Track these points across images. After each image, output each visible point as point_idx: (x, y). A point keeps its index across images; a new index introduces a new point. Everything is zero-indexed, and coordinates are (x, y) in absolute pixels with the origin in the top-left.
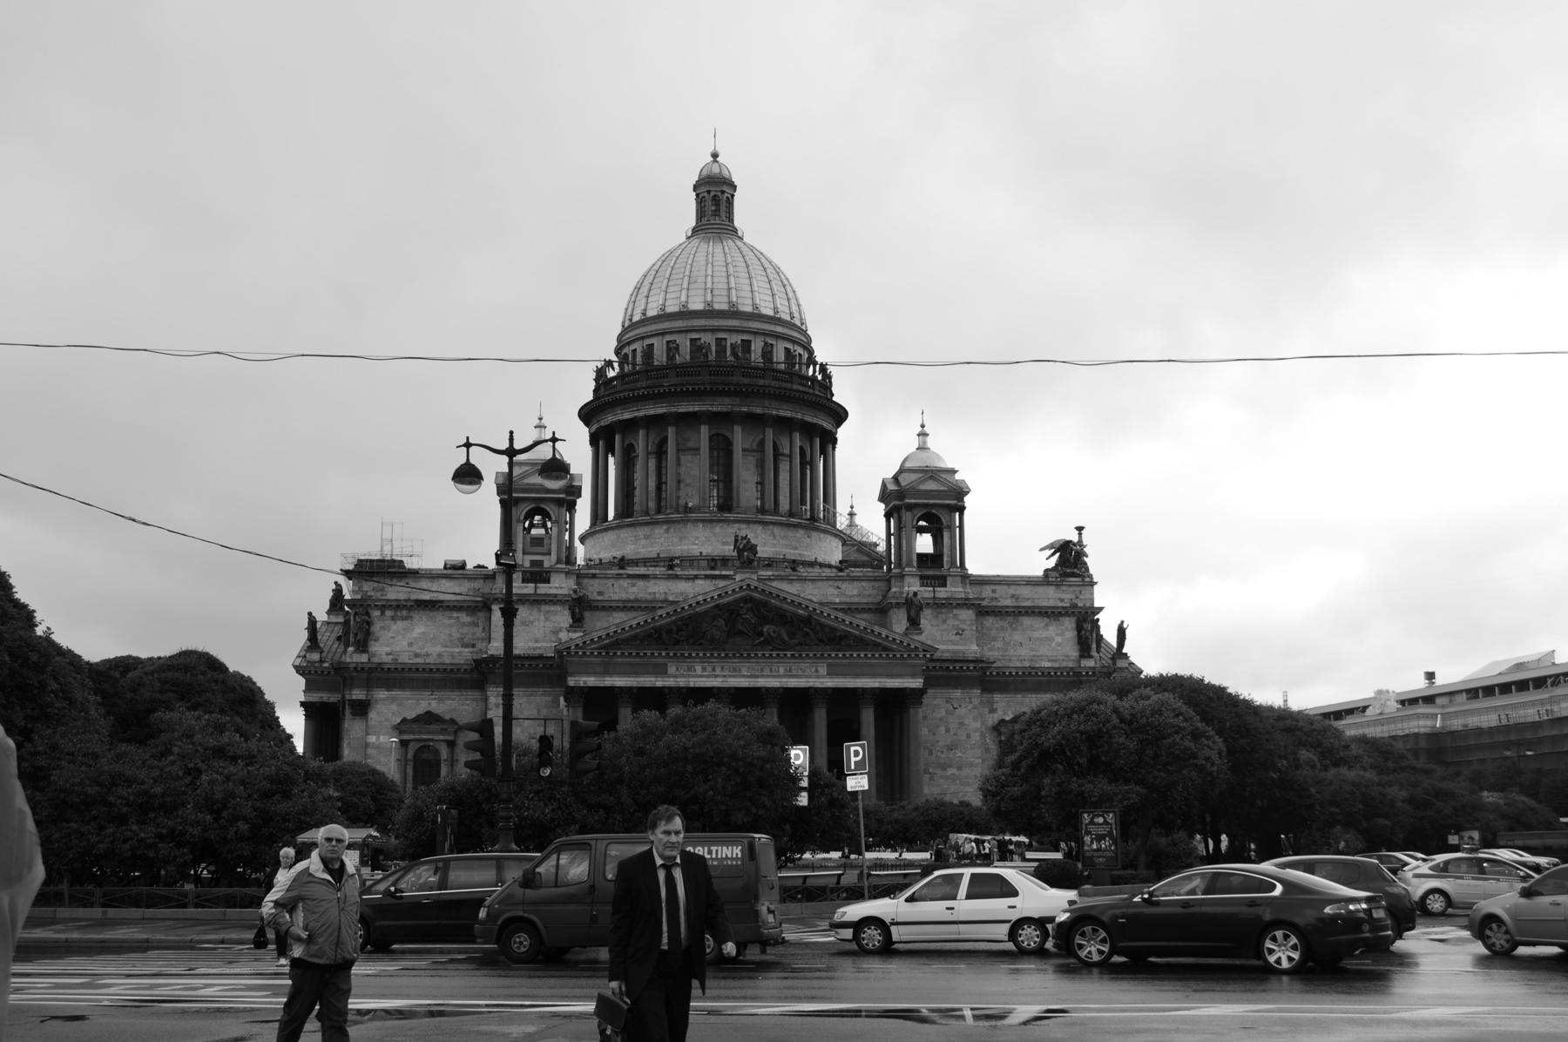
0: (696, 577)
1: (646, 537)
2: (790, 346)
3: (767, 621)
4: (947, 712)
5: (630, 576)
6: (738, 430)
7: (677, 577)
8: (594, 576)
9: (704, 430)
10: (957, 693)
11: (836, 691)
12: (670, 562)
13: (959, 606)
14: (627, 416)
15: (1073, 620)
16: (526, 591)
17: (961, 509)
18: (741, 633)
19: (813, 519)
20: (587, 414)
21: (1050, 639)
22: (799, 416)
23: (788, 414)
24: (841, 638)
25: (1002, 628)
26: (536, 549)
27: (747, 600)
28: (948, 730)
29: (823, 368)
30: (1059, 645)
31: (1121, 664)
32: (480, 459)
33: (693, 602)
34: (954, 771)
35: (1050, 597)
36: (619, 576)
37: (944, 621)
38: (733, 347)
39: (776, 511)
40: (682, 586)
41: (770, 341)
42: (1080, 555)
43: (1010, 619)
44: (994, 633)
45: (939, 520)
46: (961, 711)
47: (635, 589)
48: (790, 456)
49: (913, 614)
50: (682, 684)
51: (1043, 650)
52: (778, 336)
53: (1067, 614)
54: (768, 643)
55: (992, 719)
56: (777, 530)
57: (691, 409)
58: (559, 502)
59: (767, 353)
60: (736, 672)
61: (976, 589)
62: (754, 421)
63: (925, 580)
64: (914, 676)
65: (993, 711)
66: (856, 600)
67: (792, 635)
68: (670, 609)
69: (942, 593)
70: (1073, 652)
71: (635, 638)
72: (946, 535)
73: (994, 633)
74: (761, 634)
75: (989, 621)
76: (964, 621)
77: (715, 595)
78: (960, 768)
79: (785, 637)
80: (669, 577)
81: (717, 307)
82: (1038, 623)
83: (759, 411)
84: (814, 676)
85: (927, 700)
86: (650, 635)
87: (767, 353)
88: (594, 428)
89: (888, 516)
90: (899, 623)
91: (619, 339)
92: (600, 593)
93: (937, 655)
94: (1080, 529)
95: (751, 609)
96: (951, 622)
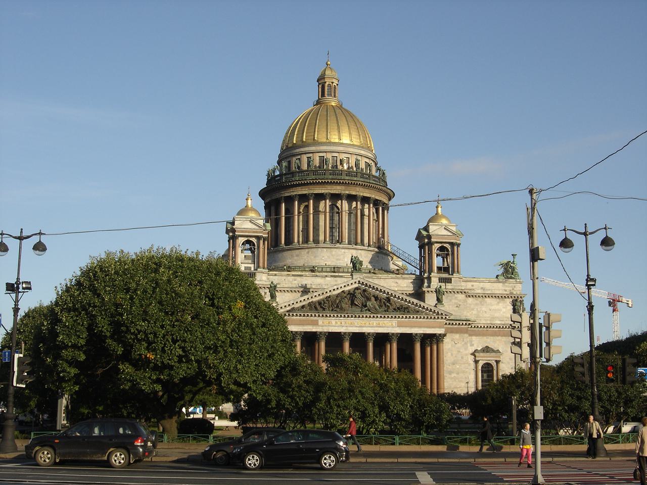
0: (326, 276)
1: (297, 256)
2: (367, 160)
3: (369, 299)
4: (452, 345)
5: (293, 275)
7: (317, 276)
8: (275, 275)
10: (457, 336)
11: (402, 334)
12: (313, 270)
14: (287, 195)
15: (511, 300)
17: (458, 245)
20: (263, 194)
21: (500, 310)
22: (373, 196)
25: (477, 304)
26: (247, 261)
27: (357, 289)
28: (452, 355)
29: (384, 174)
30: (504, 313)
32: (571, 236)
33: (331, 289)
34: (456, 375)
36: (288, 275)
37: (451, 300)
38: (341, 160)
39: (362, 243)
40: (318, 281)
41: (359, 158)
42: (513, 269)
43: (480, 299)
44: (472, 306)
45: (448, 250)
46: (459, 345)
47: (296, 282)
48: (369, 216)
49: (440, 298)
51: (497, 315)
55: (472, 350)
57: (320, 192)
58: (258, 238)
59: (357, 165)
60: (352, 325)
61: (463, 284)
62: (351, 198)
63: (441, 280)
64: (440, 327)
65: (472, 345)
66: (406, 289)
67: (380, 306)
68: (320, 293)
71: (303, 307)
73: (472, 306)
74: (366, 306)
75: (470, 300)
76: (460, 301)
78: (458, 373)
80: (313, 276)
81: (332, 140)
82: (493, 301)
83: (354, 193)
84: (390, 325)
85: (446, 340)
87: (357, 165)
88: (268, 200)
89: (421, 247)
90: (430, 300)
91: (279, 156)
93: (452, 318)
96: (454, 301)
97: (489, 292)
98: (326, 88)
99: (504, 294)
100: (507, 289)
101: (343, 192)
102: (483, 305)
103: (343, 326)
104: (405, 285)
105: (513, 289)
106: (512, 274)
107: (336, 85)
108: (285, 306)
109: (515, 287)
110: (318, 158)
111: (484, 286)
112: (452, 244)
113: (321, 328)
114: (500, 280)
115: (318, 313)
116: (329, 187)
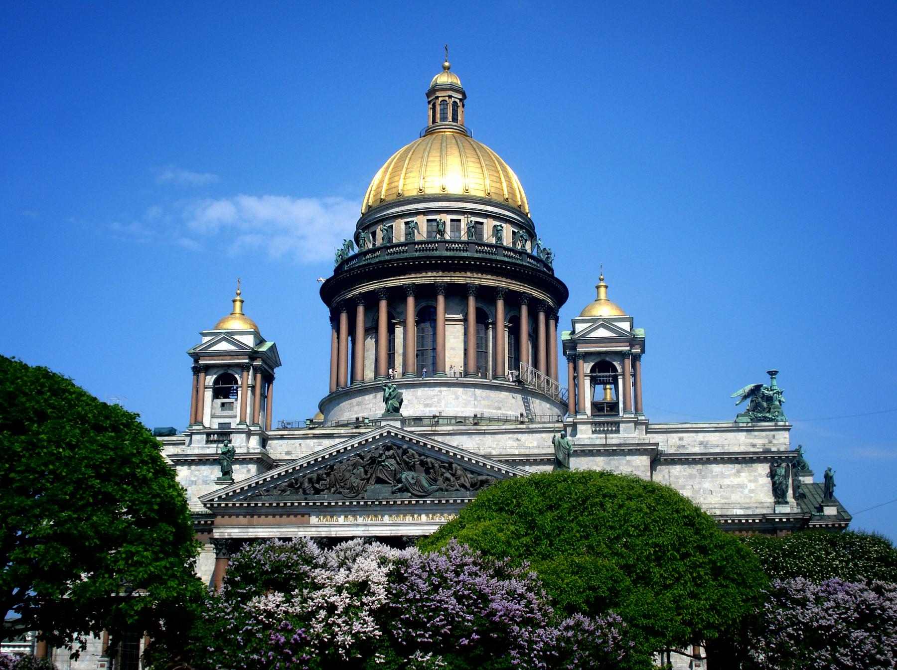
1: (358, 404)
5: (316, 437)
6: (441, 299)
8: (282, 437)
9: (411, 301)
13: (631, 452)
16: (208, 451)
17: (636, 358)
18: (379, 481)
19: (519, 381)
21: (742, 486)
22: (504, 285)
23: (492, 283)
24: (483, 483)
25: (691, 476)
30: (751, 491)
31: (830, 511)
35: (740, 442)
36: (305, 437)
43: (699, 467)
45: (615, 370)
50: (324, 534)
51: (735, 497)
52: (486, 215)
53: (759, 460)
54: (408, 490)
56: (478, 392)
63: (597, 427)
69: (614, 439)
70: (770, 499)
72: (620, 381)
77: (355, 442)
79: (425, 483)
83: (461, 281)
86: (291, 485)
92: (288, 453)
94: (772, 374)
95: (393, 457)
97: (718, 450)
98: (438, 108)
99: (749, 453)
100: (755, 441)
101: (439, 280)
102: (704, 477)
103: (357, 525)
104: (535, 444)
105: (770, 442)
106: (769, 412)
107: (458, 101)
108: (242, 489)
109: (774, 437)
110: (403, 226)
111: (706, 439)
112: (622, 355)
113: (314, 529)
114: (741, 425)
115: (306, 499)
116: (413, 275)
